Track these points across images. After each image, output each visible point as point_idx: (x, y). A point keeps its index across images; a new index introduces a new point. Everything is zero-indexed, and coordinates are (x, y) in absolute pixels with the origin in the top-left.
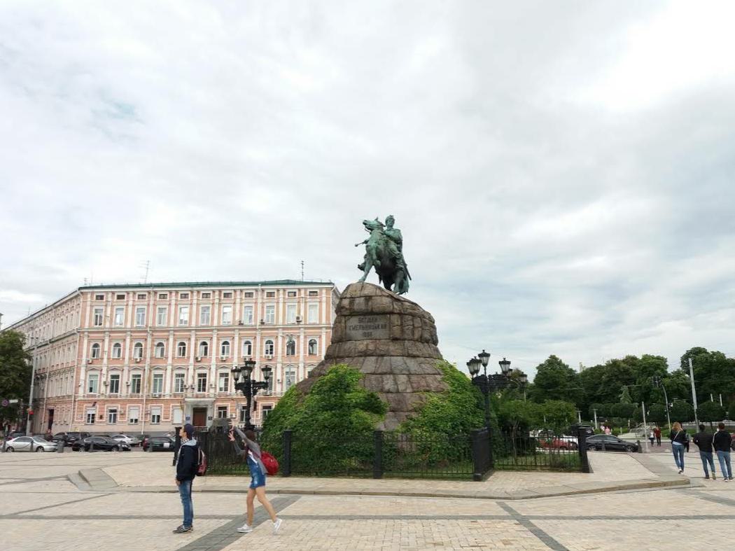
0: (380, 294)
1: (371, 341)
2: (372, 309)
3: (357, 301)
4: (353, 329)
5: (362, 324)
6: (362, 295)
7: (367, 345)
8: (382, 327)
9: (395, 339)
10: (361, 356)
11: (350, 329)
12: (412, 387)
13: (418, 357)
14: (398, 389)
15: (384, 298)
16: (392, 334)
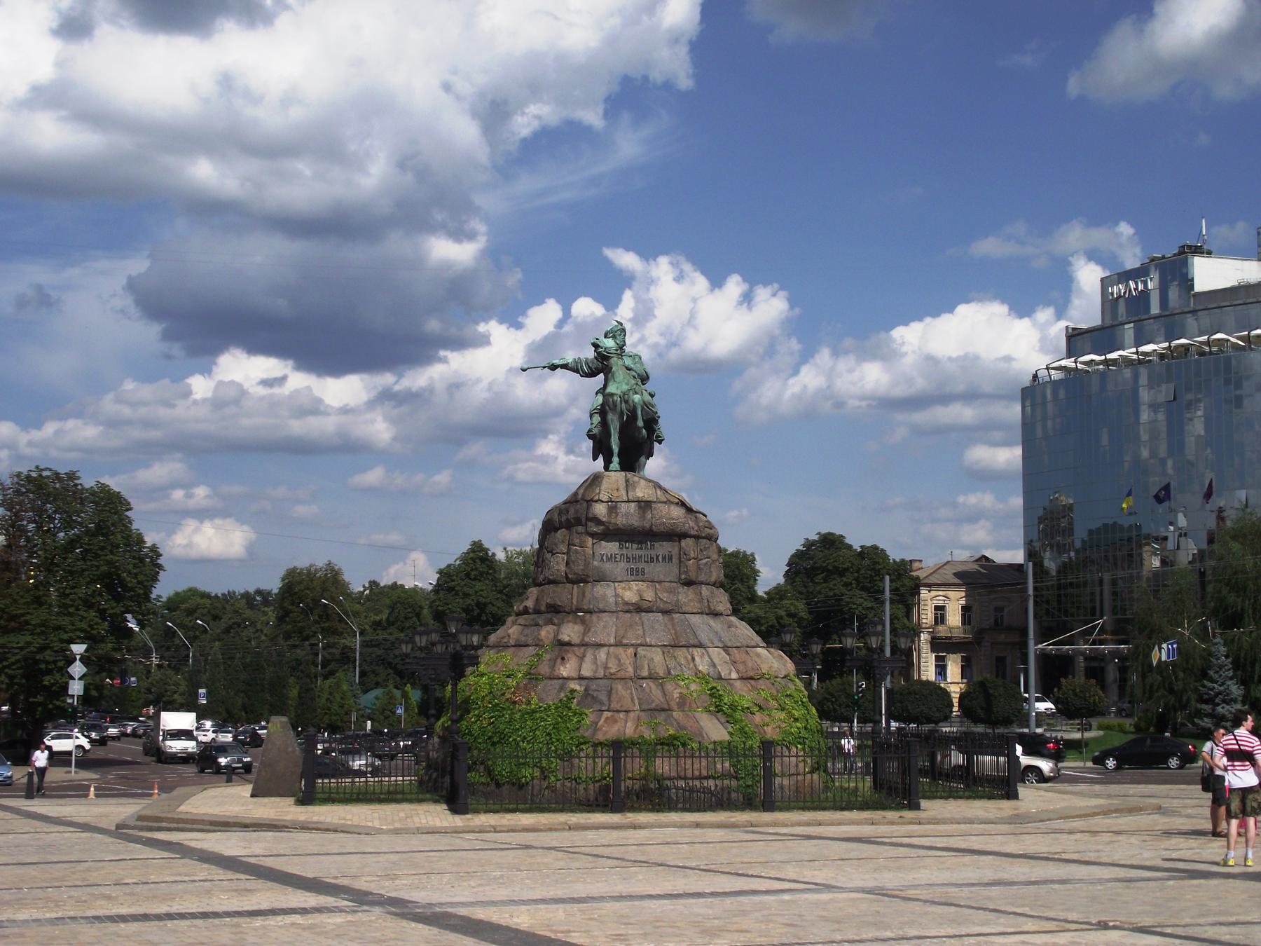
0: (665, 500)
1: (645, 584)
2: (651, 527)
3: (623, 508)
4: (609, 559)
5: (625, 551)
6: (631, 497)
7: (640, 593)
8: (664, 558)
9: (689, 583)
10: (627, 612)
11: (602, 558)
12: (738, 672)
13: (721, 614)
14: (721, 676)
15: (673, 507)
16: (686, 573)
